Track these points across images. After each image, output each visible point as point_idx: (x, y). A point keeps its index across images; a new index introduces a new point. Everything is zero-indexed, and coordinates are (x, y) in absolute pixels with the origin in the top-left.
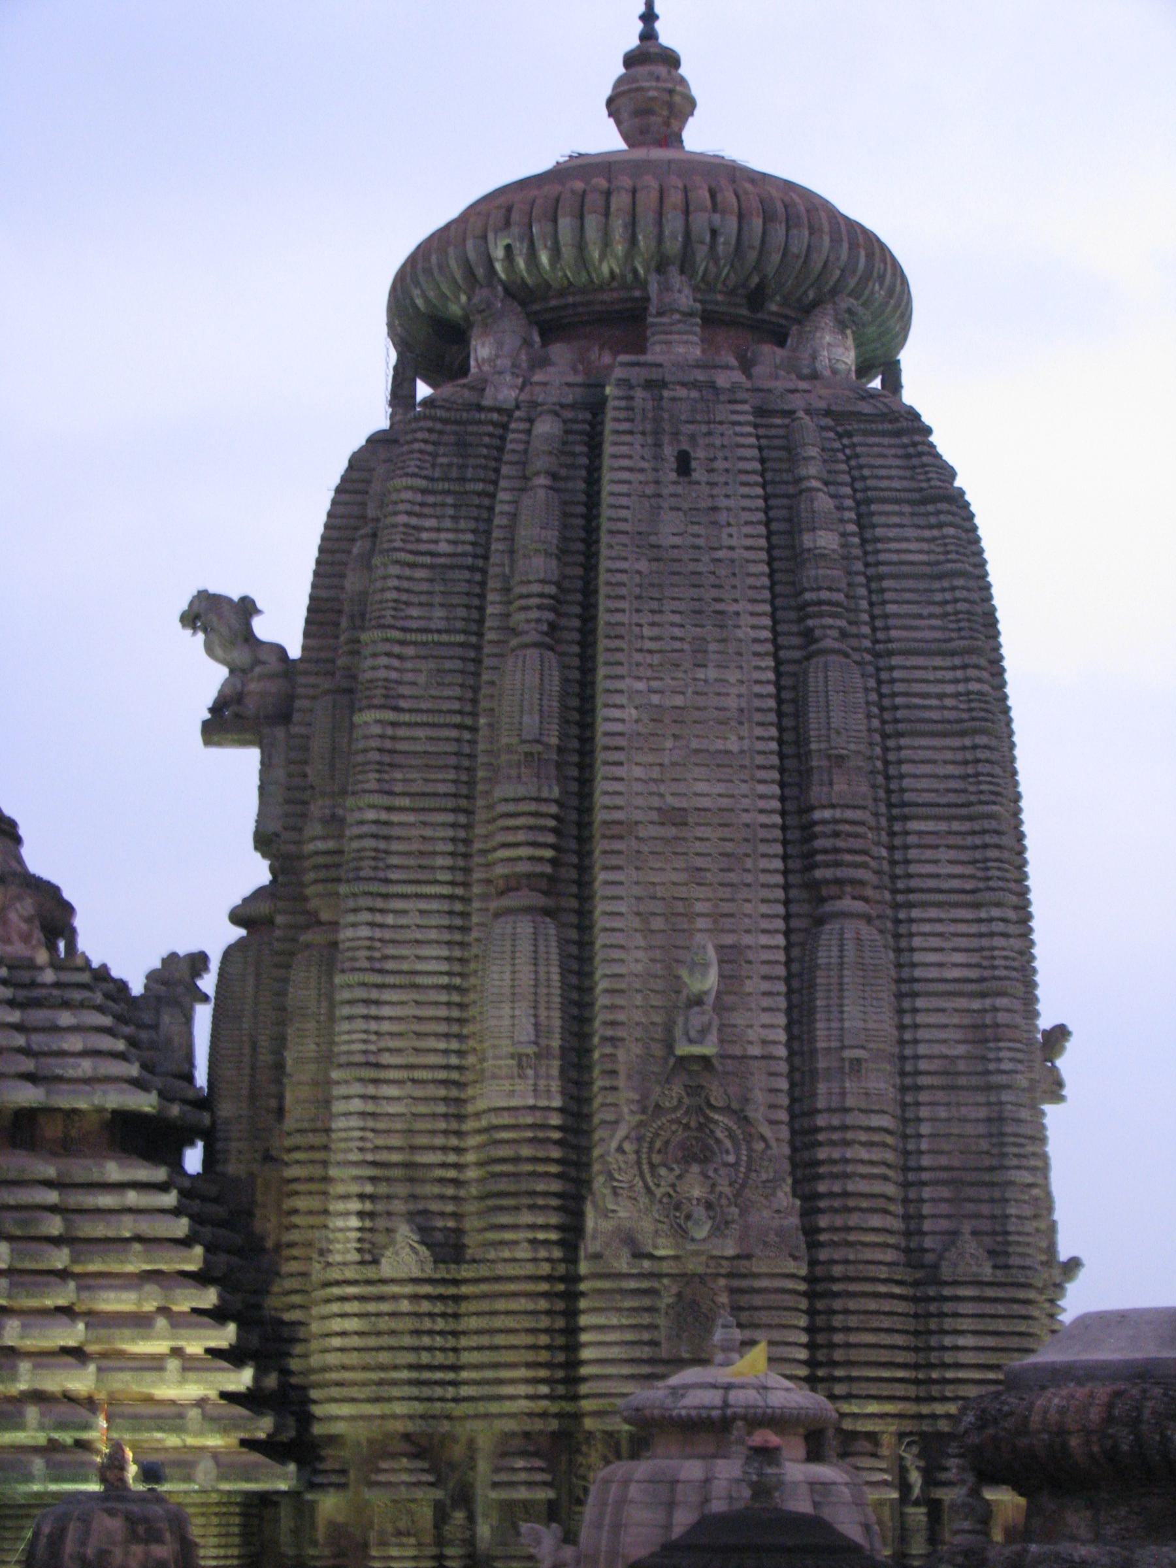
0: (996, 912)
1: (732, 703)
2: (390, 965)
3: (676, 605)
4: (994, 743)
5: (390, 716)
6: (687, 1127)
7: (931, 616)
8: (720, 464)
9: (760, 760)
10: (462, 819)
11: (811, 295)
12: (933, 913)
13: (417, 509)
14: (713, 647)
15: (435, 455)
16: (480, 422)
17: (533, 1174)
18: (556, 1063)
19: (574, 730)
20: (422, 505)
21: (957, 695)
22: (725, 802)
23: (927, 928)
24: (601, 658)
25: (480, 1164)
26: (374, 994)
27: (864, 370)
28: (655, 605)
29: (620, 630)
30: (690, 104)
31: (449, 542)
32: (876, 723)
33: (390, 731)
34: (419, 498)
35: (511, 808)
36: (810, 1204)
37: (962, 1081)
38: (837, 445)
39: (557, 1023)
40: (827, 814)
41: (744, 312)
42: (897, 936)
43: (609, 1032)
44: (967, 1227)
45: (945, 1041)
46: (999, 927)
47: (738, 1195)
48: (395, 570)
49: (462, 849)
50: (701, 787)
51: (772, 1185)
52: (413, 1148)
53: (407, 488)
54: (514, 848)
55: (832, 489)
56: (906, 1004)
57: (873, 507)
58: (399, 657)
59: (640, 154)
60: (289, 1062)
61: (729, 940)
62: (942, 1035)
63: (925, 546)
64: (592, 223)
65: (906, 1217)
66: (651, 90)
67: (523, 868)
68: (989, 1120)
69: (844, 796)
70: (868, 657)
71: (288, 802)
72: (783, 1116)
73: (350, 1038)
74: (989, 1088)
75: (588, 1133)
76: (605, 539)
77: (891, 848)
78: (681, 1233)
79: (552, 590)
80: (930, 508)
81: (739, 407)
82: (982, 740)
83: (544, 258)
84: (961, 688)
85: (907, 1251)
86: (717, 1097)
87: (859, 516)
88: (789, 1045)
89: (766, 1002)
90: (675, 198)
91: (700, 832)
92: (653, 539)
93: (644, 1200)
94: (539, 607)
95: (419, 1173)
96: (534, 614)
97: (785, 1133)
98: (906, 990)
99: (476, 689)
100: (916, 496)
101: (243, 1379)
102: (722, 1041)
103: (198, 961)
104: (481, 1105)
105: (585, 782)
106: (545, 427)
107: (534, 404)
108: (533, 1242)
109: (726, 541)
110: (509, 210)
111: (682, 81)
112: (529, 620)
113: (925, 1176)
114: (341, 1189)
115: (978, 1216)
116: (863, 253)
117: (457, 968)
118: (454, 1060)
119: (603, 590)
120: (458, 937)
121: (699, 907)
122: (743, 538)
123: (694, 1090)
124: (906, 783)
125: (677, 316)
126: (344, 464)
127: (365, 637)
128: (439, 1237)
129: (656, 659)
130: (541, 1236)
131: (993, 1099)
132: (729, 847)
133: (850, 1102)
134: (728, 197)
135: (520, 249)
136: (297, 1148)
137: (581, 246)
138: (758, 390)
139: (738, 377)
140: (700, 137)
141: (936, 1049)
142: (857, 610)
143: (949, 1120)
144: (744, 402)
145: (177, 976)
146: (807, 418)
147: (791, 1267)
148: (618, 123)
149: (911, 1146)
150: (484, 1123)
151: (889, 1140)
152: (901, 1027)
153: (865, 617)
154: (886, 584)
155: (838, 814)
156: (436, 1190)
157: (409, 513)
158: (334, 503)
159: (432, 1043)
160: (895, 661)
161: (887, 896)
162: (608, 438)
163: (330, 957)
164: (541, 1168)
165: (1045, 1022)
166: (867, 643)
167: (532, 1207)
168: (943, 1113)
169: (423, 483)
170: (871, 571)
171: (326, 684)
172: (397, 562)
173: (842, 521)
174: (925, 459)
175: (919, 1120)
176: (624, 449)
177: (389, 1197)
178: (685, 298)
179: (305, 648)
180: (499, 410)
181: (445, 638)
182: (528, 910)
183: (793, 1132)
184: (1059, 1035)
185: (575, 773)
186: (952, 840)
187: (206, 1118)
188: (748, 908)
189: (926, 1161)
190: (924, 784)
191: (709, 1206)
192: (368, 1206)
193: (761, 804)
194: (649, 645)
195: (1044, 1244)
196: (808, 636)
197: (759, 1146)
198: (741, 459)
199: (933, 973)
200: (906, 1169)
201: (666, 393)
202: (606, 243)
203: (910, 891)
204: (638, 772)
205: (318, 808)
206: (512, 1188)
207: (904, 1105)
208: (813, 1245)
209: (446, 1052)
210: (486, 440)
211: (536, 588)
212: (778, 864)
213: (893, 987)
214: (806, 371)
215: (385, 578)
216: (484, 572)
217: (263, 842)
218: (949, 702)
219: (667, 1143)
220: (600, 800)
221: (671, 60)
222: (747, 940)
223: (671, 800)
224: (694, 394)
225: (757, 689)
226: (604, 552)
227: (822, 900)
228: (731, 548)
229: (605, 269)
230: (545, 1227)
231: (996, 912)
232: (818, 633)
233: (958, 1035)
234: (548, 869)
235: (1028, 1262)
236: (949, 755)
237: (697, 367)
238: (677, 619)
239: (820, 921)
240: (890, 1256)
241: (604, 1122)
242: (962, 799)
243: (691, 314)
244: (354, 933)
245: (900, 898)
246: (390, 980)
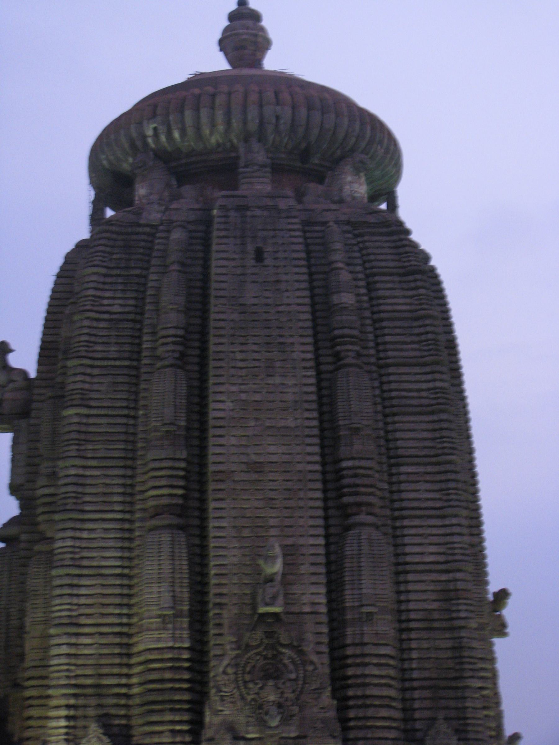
0: (454, 521)
1: (289, 397)
2: (85, 563)
3: (256, 340)
4: (452, 418)
5: (84, 411)
6: (265, 658)
7: (413, 343)
8: (281, 255)
9: (307, 432)
10: (129, 472)
11: (339, 152)
12: (416, 522)
13: (101, 286)
14: (278, 364)
15: (111, 253)
16: (138, 233)
17: (172, 689)
18: (186, 620)
19: (195, 417)
20: (104, 283)
21: (428, 390)
22: (285, 458)
23: (413, 531)
24: (211, 372)
25: (141, 684)
26: (75, 581)
27: (374, 198)
28: (242, 340)
29: (221, 356)
31: (121, 305)
32: (379, 408)
33: (84, 421)
34: (102, 279)
35: (156, 465)
36: (343, 704)
37: (436, 625)
38: (354, 242)
39: (186, 595)
40: (349, 463)
41: (299, 164)
42: (395, 537)
43: (218, 600)
44: (441, 715)
45: (424, 601)
46: (456, 530)
47: (297, 698)
48: (87, 323)
49: (129, 490)
50: (272, 449)
51: (319, 690)
52: (101, 676)
53: (95, 274)
54: (158, 490)
55: (351, 268)
56: (402, 578)
57: (377, 278)
58: (89, 375)
59: (237, 72)
60: (28, 624)
61: (290, 541)
62: (424, 596)
63: (408, 301)
64: (204, 113)
65: (404, 710)
66: (244, 35)
67: (165, 501)
68: (454, 648)
70: (374, 368)
71: (29, 465)
72: (325, 649)
73: (61, 608)
74: (452, 629)
75: (206, 663)
76: (213, 301)
77: (391, 483)
78: (262, 724)
79: (180, 332)
80: (411, 278)
81: (293, 220)
82: (444, 416)
83: (176, 135)
84: (431, 385)
85: (405, 731)
86: (284, 638)
87: (368, 284)
89: (314, 579)
90: (253, 97)
91: (271, 476)
92: (241, 301)
93: (240, 704)
94: (174, 343)
95: (104, 691)
96: (171, 347)
97: (326, 659)
98: (400, 569)
99: (136, 393)
100: (401, 271)
102: (286, 604)
104: (141, 647)
105: (203, 448)
106: (177, 235)
107: (171, 222)
108: (172, 731)
109: (286, 301)
110: (156, 106)
111: (262, 29)
113: (416, 684)
114: (54, 702)
115: (447, 708)
116: (369, 128)
117: (126, 564)
118: (125, 620)
119: (212, 332)
120: (127, 544)
122: (295, 299)
123: (269, 635)
124: (399, 443)
125: (256, 168)
126: (59, 261)
127: (70, 363)
128: (115, 730)
129: (243, 372)
130: (178, 728)
131: (456, 635)
132: (289, 485)
133: (366, 639)
134: (286, 96)
135: (162, 129)
136: (30, 679)
137: (198, 128)
138: (307, 210)
139: (292, 202)
140: (272, 62)
141: (421, 606)
142: (367, 340)
143: (428, 649)
144: (295, 217)
146: (335, 227)
148: (226, 55)
149: (406, 666)
150: (142, 658)
151: (392, 662)
152: (399, 593)
153: (371, 344)
154: (385, 324)
155: (357, 463)
156: (114, 701)
157: (96, 289)
158: (56, 283)
159: (111, 610)
160: (391, 370)
161: (388, 512)
162: (215, 241)
163: (50, 560)
164: (177, 686)
165: (493, 587)
166: (373, 360)
167: (172, 710)
168: (425, 645)
169: (103, 271)
170: (376, 316)
171: (49, 393)
172: (87, 318)
173: (357, 287)
174: (407, 249)
175: (411, 649)
176: (223, 247)
177: (85, 706)
178: (261, 157)
179: (39, 372)
180: (152, 226)
181: (118, 363)
182: (169, 526)
183: (333, 659)
184: (502, 596)
185: (196, 442)
186: (428, 478)
188: (301, 522)
189: (415, 675)
190: (411, 444)
191: (280, 706)
192: (72, 713)
193: (309, 458)
194: (240, 364)
195: (493, 725)
196: (337, 356)
197: (310, 668)
198: (294, 251)
199: (417, 559)
200: (403, 680)
201: (249, 213)
202: (213, 125)
203: (402, 509)
204: (234, 441)
205: (45, 467)
206: (160, 698)
207: (401, 641)
208: (345, 729)
209: (120, 615)
210: (143, 244)
211: (171, 332)
212: (319, 495)
213: (393, 568)
214: (336, 198)
215: (81, 327)
216: (140, 322)
218: (424, 394)
219: (254, 667)
220: (211, 459)
221: (256, 17)
222: (301, 541)
223: (254, 458)
224: (265, 213)
225: (306, 389)
226: (213, 309)
227: (348, 516)
228: (288, 305)
229: (213, 140)
230: (180, 722)
231: (454, 521)
232: (343, 354)
233: (433, 596)
234: (180, 501)
235: (480, 736)
236: (424, 426)
237: (267, 197)
238: (256, 348)
239: (347, 528)
241: (216, 656)
242: (433, 452)
243: (264, 166)
244: (63, 544)
245: (397, 513)
246: (85, 572)
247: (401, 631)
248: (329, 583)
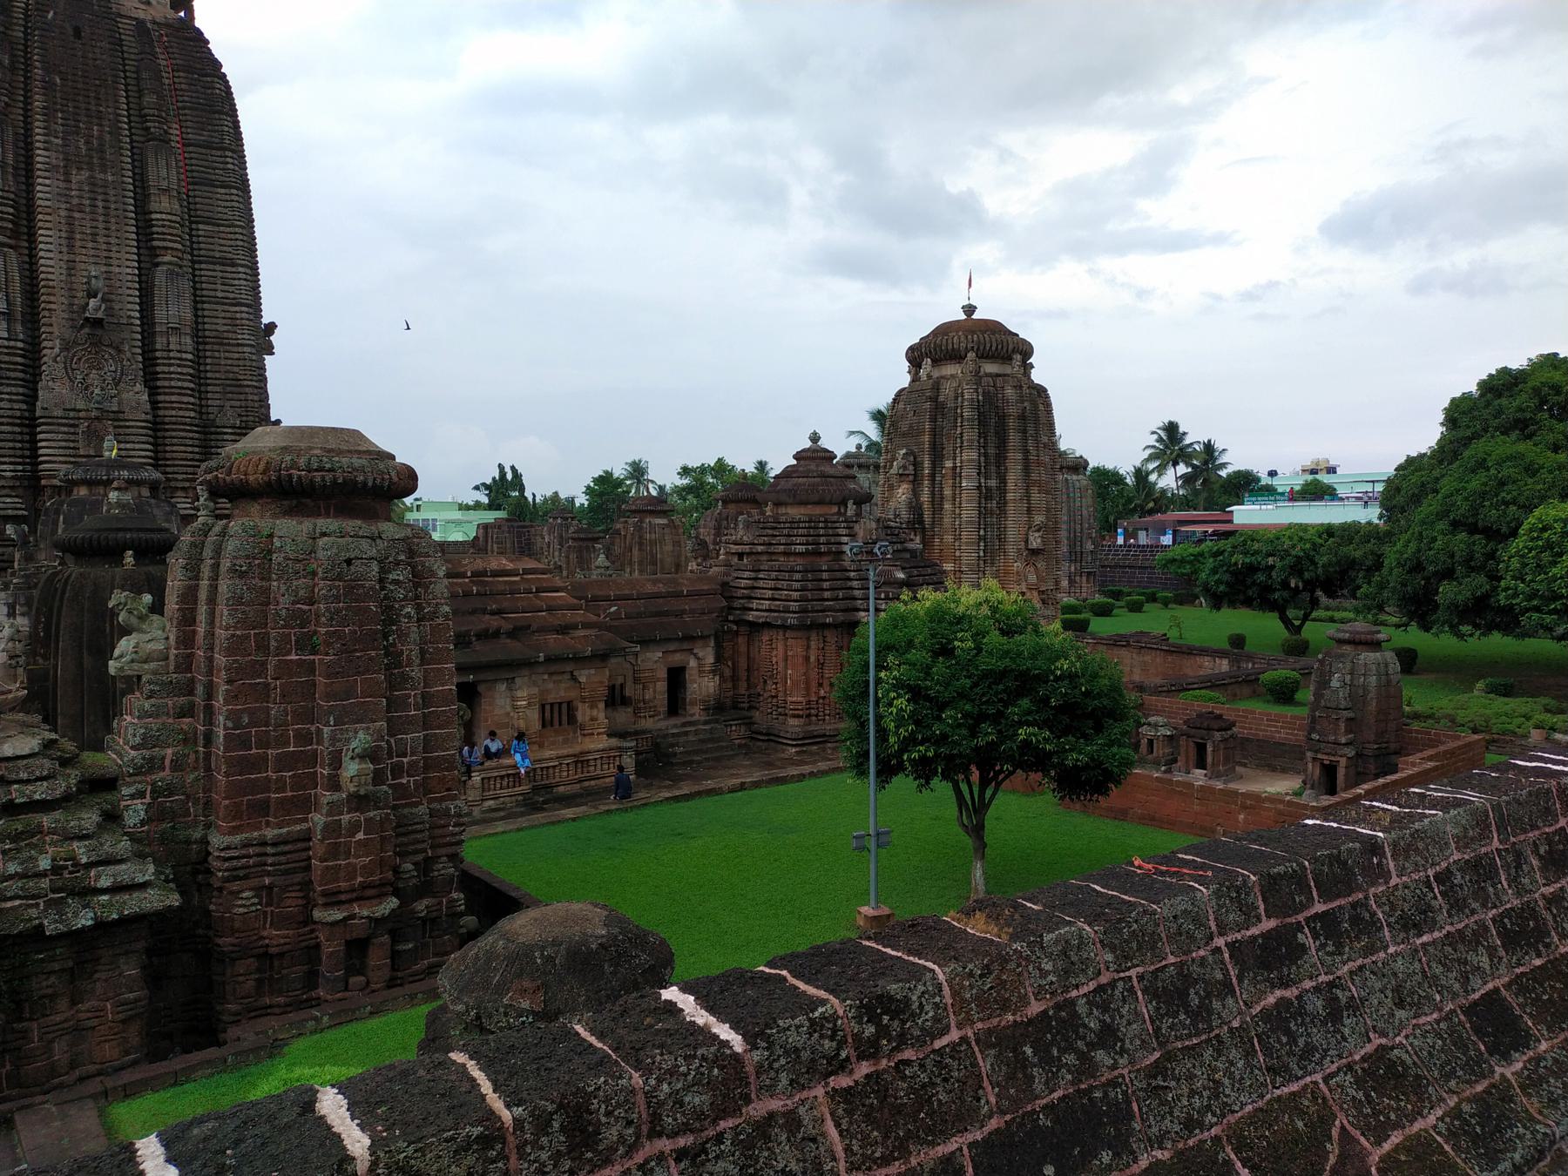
36: (153, 391)
69: (164, 207)
88: (141, 318)
97: (140, 358)
147: (143, 417)
165: (265, 320)
239: (157, 265)
240: (192, 414)
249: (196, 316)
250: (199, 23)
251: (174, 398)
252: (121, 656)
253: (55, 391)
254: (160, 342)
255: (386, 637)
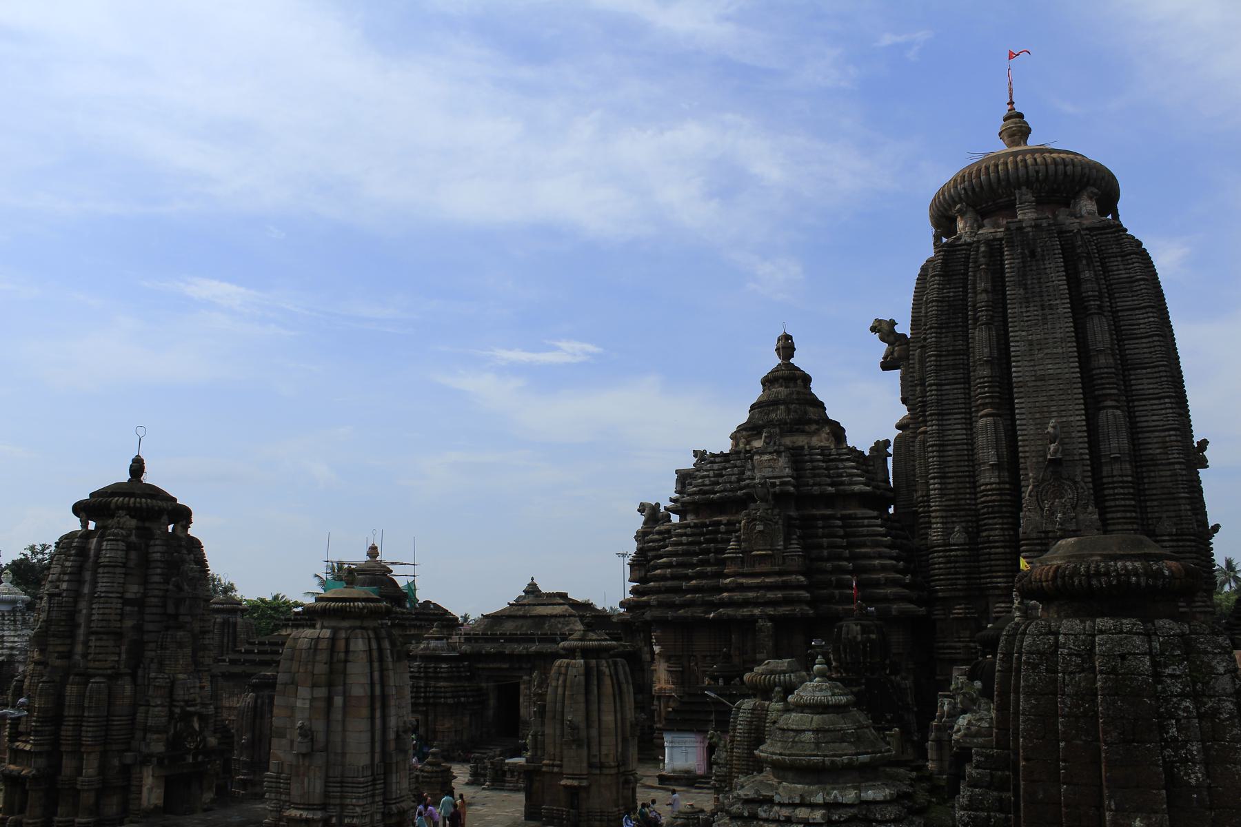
27: (1103, 212)
30: (1029, 130)
36: (1103, 511)
98: (1134, 431)
101: (908, 578)
103: (887, 443)
112: (983, 316)
121: (1053, 408)
122: (1056, 278)
145: (880, 447)
187: (891, 495)
217: (904, 401)
221: (1020, 116)
239: (1100, 409)
247: (1137, 467)
248: (1089, 442)
249: (1134, 445)
250: (1124, 220)
251: (1119, 515)
252: (959, 730)
253: (1029, 519)
254: (1106, 470)
255: (1163, 728)
